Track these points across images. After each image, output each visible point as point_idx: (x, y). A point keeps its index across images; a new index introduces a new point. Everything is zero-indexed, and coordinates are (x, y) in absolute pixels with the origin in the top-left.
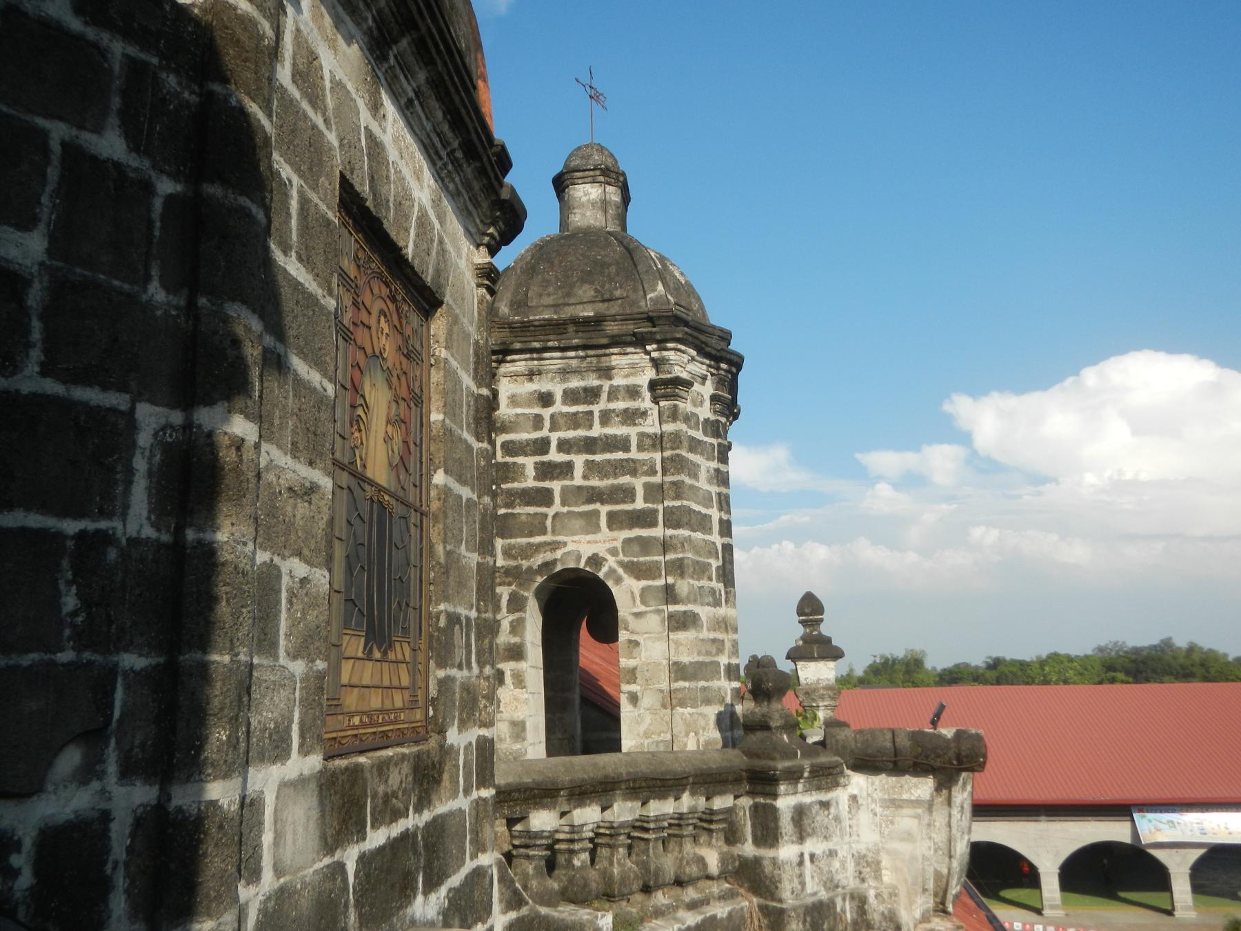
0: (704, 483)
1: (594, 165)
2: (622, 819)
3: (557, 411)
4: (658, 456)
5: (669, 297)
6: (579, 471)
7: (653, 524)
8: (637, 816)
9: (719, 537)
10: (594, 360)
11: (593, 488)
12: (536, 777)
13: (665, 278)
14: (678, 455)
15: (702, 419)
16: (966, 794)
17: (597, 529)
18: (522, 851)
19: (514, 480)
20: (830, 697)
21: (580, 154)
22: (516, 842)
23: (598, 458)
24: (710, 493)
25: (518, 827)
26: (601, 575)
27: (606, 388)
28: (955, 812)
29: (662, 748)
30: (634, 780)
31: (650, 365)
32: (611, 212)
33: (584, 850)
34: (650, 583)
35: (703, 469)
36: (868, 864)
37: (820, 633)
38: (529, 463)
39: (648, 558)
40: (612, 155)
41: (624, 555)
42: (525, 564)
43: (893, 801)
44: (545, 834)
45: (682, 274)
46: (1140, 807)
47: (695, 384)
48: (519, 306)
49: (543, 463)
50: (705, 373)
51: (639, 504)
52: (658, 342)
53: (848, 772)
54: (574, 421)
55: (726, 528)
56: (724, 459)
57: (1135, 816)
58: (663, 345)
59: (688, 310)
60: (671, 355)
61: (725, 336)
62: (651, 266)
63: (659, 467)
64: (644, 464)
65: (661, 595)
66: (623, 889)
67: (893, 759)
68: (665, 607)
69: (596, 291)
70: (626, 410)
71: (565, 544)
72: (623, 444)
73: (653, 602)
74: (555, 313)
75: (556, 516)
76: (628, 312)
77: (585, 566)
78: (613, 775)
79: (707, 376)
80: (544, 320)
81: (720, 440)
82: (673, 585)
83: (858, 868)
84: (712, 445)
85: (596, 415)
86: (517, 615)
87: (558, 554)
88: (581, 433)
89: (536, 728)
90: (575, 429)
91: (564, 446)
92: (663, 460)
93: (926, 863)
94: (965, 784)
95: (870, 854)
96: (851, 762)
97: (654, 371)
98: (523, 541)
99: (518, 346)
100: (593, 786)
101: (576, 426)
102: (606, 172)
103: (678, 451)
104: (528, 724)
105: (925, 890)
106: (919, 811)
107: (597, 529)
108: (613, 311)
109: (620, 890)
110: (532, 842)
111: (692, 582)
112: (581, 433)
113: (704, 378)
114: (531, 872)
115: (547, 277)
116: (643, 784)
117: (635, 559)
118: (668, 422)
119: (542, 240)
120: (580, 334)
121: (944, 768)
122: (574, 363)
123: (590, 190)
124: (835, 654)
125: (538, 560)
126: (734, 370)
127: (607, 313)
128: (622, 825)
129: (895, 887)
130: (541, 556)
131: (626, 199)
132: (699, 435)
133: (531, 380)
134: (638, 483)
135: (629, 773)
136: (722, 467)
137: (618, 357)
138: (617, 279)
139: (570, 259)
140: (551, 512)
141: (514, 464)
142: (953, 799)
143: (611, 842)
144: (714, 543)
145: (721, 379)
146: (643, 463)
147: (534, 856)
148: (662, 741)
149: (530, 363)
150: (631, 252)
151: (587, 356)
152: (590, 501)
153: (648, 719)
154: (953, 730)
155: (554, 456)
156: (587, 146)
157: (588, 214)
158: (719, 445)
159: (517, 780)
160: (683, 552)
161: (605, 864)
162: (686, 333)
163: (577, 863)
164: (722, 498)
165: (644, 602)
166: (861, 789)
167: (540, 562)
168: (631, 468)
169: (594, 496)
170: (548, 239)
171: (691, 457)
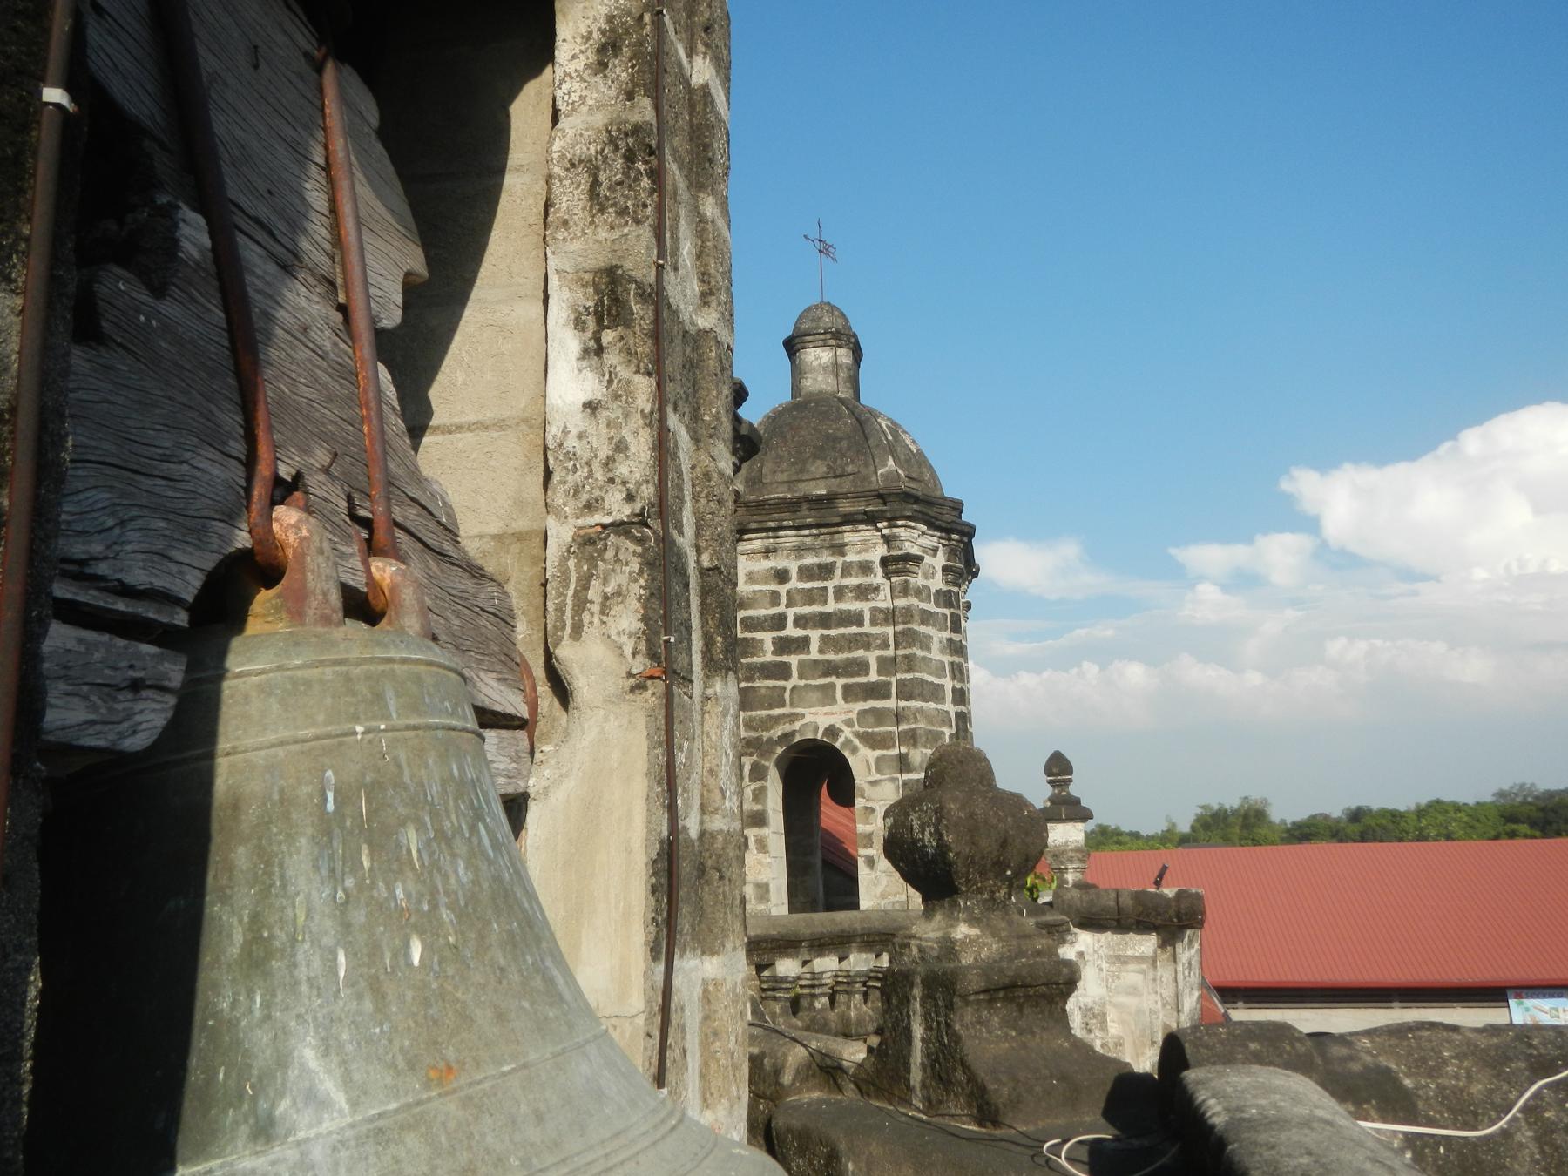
0: (936, 654)
1: (825, 329)
2: (857, 969)
3: (793, 587)
4: (890, 630)
5: (900, 471)
6: (815, 645)
7: (887, 696)
8: (871, 967)
9: (951, 706)
10: (828, 537)
11: (829, 662)
12: (780, 930)
13: (896, 451)
14: (909, 629)
15: (933, 591)
16: (1193, 952)
17: (833, 701)
18: (770, 993)
19: (753, 655)
20: (1079, 859)
21: (810, 315)
22: (765, 986)
23: (833, 632)
24: (943, 663)
25: (766, 973)
26: (838, 745)
27: (839, 565)
28: (1180, 968)
29: (897, 907)
30: (869, 935)
31: (881, 541)
32: (843, 375)
33: (824, 994)
34: (884, 752)
35: (935, 640)
36: (1095, 1016)
37: (1068, 793)
38: (767, 637)
39: (882, 729)
40: (843, 315)
41: (860, 726)
42: (765, 735)
43: (1118, 957)
44: (790, 979)
45: (914, 442)
46: (1518, 991)
47: (926, 556)
48: (754, 483)
49: (781, 638)
50: (936, 544)
51: (873, 677)
52: (889, 520)
53: (1076, 930)
54: (809, 597)
55: (961, 697)
56: (956, 627)
57: (1512, 1002)
58: (893, 522)
59: (920, 481)
60: (901, 532)
61: (956, 506)
62: (881, 440)
63: (891, 641)
64: (877, 639)
65: (895, 764)
66: (859, 1029)
67: (1116, 917)
68: (899, 775)
69: (829, 467)
70: (859, 586)
71: (803, 716)
72: (857, 619)
73: (887, 771)
74: (790, 490)
75: (794, 688)
76: (859, 490)
77: (823, 737)
78: (848, 929)
79: (937, 548)
80: (778, 498)
81: (952, 610)
82: (907, 754)
83: (1085, 1020)
84: (945, 615)
85: (831, 591)
86: (759, 784)
87: (797, 726)
88: (816, 608)
89: (779, 890)
90: (810, 605)
91: (800, 621)
92: (895, 634)
93: (1153, 1016)
94: (1191, 941)
95: (1097, 1007)
96: (1077, 920)
97: (886, 547)
98: (763, 713)
99: (754, 525)
100: (832, 939)
101: (811, 602)
102: (837, 335)
103: (909, 626)
104: (772, 887)
105: (1153, 1043)
106: (1144, 966)
107: (833, 701)
108: (844, 490)
109: (856, 1030)
110: (779, 985)
111: (924, 751)
112: (816, 608)
113: (935, 550)
114: (778, 1011)
115: (780, 452)
116: (877, 938)
117: (870, 730)
118: (900, 597)
119: (774, 411)
120: (813, 513)
121: (1166, 925)
122: (808, 540)
123: (821, 354)
124: (1085, 816)
125: (778, 731)
126: (966, 539)
127: (840, 491)
128: (858, 974)
129: (1121, 1038)
130: (781, 727)
131: (857, 354)
132: (931, 607)
133: (768, 557)
134: (872, 657)
135: (863, 929)
136: (956, 637)
137: (850, 534)
138: (848, 454)
139: (803, 433)
140: (789, 685)
141: (753, 639)
142: (1178, 956)
143: (848, 989)
144: (947, 712)
145: (952, 550)
146: (877, 637)
147: (780, 997)
148: (898, 902)
149: (765, 541)
150: (863, 422)
151: (818, 535)
152: (826, 674)
153: (884, 881)
154: (1175, 890)
155: (791, 631)
156: (816, 307)
157: (820, 378)
158: (952, 614)
159: (764, 932)
160: (916, 721)
161: (843, 1008)
162: (916, 511)
163: (818, 1005)
164: (956, 667)
165: (878, 770)
166: (1088, 947)
167: (779, 733)
168: (865, 642)
169: (830, 669)
170: (780, 409)
171: (923, 629)
